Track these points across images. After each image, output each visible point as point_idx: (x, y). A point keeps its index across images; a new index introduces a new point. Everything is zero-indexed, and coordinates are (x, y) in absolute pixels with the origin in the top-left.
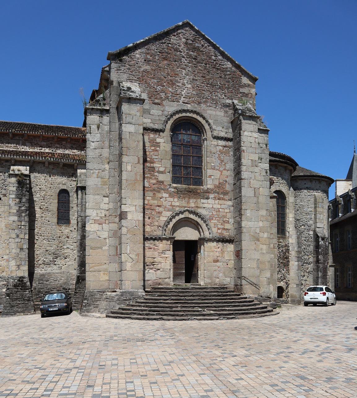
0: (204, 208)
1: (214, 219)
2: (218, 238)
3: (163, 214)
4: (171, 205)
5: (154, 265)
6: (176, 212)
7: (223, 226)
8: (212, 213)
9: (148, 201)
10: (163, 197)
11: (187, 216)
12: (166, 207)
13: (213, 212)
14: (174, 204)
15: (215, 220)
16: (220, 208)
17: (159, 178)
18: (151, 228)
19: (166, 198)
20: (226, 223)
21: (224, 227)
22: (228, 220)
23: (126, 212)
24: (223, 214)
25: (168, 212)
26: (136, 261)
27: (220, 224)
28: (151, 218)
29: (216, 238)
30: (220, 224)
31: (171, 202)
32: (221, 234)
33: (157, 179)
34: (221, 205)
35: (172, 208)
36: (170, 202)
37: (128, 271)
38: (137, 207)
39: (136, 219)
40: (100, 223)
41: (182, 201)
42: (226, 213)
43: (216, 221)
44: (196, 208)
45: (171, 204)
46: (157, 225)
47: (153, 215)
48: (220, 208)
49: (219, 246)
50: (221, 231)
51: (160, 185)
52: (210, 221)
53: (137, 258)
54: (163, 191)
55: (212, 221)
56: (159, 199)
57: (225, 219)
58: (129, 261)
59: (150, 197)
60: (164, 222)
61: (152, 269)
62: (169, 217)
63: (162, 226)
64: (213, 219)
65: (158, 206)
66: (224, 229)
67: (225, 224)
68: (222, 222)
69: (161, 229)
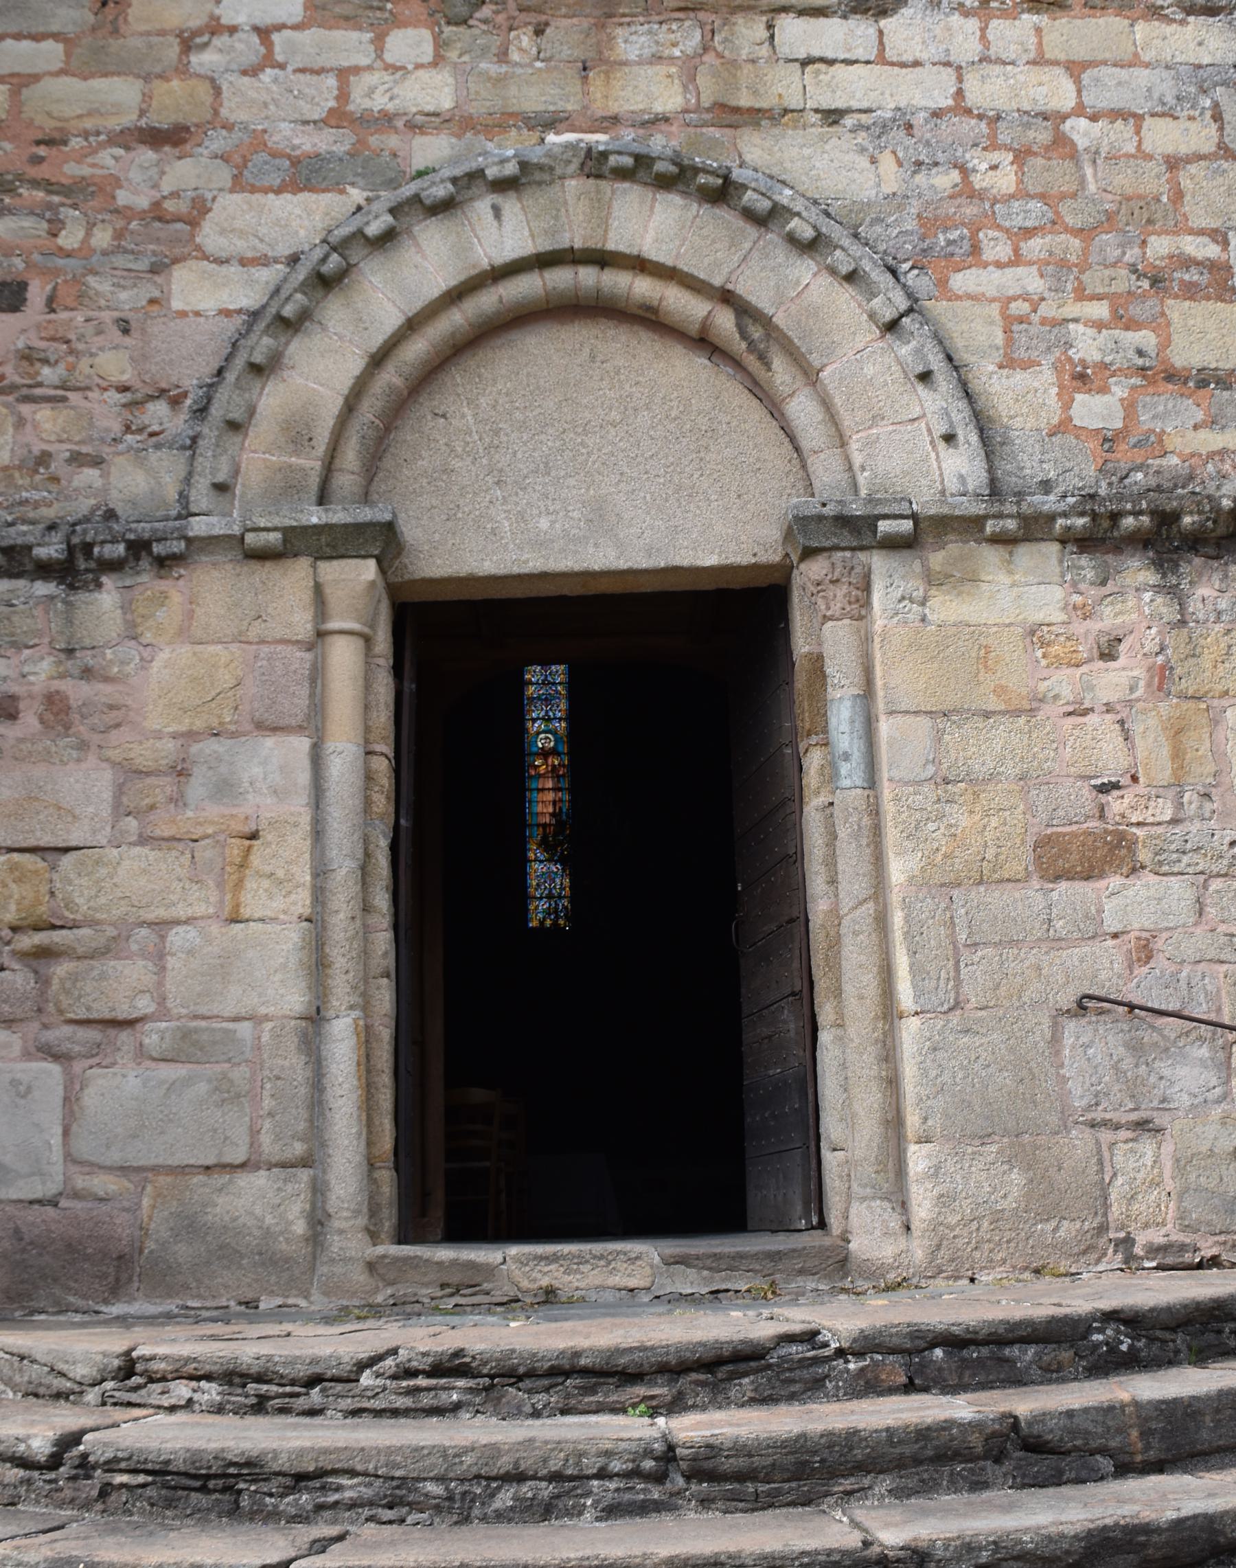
0: (833, 116)
1: (996, 247)
2: (1092, 497)
3: (210, 236)
5: (45, 953)
6: (408, 190)
7: (1146, 338)
8: (955, 176)
9: (15, 93)
10: (215, 28)
11: (576, 237)
12: (259, 141)
13: (979, 161)
14: (380, 102)
15: (1017, 260)
16: (1079, 110)
18: (20, 423)
19: (264, 33)
20: (1191, 292)
21: (1165, 343)
22: (1212, 251)
24: (1123, 180)
27: (1101, 310)
29: (1049, 503)
30: (1101, 310)
31: (344, 74)
32: (1124, 455)
34: (1075, 69)
35: (361, 142)
41: (502, 56)
42: (1173, 163)
43: (1034, 283)
44: (715, 132)
45: (343, 95)
46: (125, 378)
47: (68, 255)
48: (1079, 110)
49: (1109, 619)
50: (1130, 407)
52: (942, 283)
55: (961, 281)
56: (173, 50)
57: (1160, 247)
59: (56, 36)
62: (294, 260)
63: (190, 383)
64: (976, 249)
65: (155, 138)
66: (1171, 376)
67: (1177, 309)
68: (1124, 282)
69: (175, 423)
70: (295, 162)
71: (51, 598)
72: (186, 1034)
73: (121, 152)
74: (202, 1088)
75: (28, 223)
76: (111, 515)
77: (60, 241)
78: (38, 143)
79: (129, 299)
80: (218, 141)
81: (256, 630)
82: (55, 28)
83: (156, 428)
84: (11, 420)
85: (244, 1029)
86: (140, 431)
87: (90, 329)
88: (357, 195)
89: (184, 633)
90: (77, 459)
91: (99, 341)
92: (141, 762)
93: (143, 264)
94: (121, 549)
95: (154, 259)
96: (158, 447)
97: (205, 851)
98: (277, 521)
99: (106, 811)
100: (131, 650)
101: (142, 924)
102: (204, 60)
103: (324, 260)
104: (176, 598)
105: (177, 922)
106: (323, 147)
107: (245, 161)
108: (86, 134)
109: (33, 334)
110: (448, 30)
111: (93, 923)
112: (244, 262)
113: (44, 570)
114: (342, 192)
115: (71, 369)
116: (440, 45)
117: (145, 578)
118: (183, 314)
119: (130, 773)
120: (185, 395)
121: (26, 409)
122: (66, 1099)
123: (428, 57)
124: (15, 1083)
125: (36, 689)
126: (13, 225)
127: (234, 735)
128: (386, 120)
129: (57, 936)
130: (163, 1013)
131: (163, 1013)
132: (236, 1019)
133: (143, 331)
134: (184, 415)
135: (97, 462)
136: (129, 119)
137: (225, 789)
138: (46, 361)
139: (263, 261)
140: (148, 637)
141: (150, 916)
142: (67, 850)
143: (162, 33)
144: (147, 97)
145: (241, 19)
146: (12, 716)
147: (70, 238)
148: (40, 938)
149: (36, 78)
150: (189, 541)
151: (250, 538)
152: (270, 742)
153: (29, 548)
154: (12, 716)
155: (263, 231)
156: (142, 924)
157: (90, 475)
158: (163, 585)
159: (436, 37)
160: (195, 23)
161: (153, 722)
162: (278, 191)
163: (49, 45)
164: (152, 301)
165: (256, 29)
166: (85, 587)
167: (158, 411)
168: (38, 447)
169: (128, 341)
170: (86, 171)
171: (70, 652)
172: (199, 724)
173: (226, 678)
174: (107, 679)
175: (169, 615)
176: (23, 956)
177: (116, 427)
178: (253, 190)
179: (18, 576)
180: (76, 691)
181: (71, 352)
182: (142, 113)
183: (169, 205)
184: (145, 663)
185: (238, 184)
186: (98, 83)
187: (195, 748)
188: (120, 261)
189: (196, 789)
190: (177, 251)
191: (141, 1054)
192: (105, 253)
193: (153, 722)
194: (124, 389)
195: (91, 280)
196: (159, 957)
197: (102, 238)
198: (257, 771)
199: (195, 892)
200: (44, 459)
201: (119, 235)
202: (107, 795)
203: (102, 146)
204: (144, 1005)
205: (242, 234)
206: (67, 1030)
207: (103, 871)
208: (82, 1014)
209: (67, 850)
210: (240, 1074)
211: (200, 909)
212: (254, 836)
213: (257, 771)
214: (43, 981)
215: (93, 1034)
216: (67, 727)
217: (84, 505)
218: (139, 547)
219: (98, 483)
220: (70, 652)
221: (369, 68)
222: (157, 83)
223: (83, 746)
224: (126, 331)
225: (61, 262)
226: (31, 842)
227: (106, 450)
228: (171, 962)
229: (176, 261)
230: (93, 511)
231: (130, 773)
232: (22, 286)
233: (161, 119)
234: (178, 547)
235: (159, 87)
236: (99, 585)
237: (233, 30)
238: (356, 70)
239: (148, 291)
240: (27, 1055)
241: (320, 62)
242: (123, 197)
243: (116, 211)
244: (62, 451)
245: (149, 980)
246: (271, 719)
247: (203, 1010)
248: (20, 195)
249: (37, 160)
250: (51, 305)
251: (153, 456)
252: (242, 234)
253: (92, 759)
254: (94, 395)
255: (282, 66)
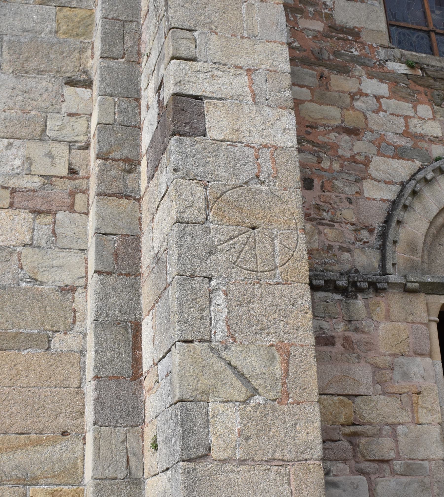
3: (372, 171)
4: (406, 133)
5: (355, 434)
10: (361, 93)
12: (382, 138)
14: (419, 130)
17: (336, 16)
18: (320, 233)
19: (378, 98)
23: (196, 97)
25: (396, 163)
26: (272, 395)
28: (317, 183)
31: (406, 118)
33: (329, 17)
36: (402, 120)
37: (224, 461)
38: (259, 79)
39: (256, 139)
40: (44, 207)
45: (407, 126)
46: (354, 220)
51: (342, 43)
53: (279, 372)
54: (359, 70)
58: (224, 393)
59: (307, 87)
60: (387, 205)
61: (345, 461)
62: (403, 185)
70: (396, 148)
71: (341, 300)
72: (408, 465)
73: (337, 135)
74: (416, 485)
75: (310, 156)
76: (357, 271)
77: (322, 165)
78: (308, 126)
79: (350, 190)
80: (368, 136)
81: (410, 318)
82: (306, 84)
83: (365, 240)
84: (316, 231)
85: (426, 463)
86: (361, 240)
87: (338, 200)
88: (418, 164)
89: (387, 318)
90: (342, 249)
91: (341, 205)
92: (381, 365)
93: (352, 178)
94: (322, 282)
95: (355, 177)
96: (369, 247)
97: (405, 398)
98: (417, 280)
99: (370, 383)
100: (369, 322)
101: (387, 424)
102: (358, 104)
103: (415, 186)
104: (383, 304)
105: (399, 424)
106: (404, 144)
107: (380, 145)
108: (324, 126)
109: (317, 199)
110: (436, 107)
111: (371, 424)
112: (386, 182)
113: (337, 289)
114: (413, 161)
115: (334, 214)
116: (434, 112)
117: (371, 296)
118: (369, 199)
119: (377, 368)
120: (374, 229)
121: (321, 228)
122: (370, 490)
123: (431, 117)
124: (352, 483)
125: (340, 334)
126: (304, 157)
127: (408, 356)
128: (421, 137)
129: (359, 428)
130: (398, 458)
131: (398, 458)
132: (423, 460)
133: (356, 203)
134: (375, 237)
135: (349, 251)
136: (338, 123)
137: (406, 375)
138: (324, 210)
139: (391, 183)
140: (375, 318)
141: (390, 422)
142: (356, 396)
143: (343, 92)
144: (342, 115)
145: (369, 92)
146: (333, 344)
147: (325, 164)
148: (352, 429)
149: (303, 102)
150: (388, 283)
151: (409, 285)
152: (419, 359)
153: (335, 281)
154: (333, 344)
155: (390, 172)
156: (387, 424)
157: (347, 255)
158: (378, 299)
159: (432, 109)
160: (354, 90)
161: (382, 350)
162: (393, 158)
163: (304, 89)
164: (357, 193)
165: (375, 96)
166: (351, 297)
167: (364, 234)
168: (327, 243)
169: (351, 206)
170: (327, 140)
171: (350, 321)
172: (397, 352)
173: (404, 335)
174: (363, 332)
175: (381, 310)
176: (345, 435)
177: (353, 239)
178: (384, 156)
179: (328, 291)
180: (355, 336)
181: (333, 208)
182: (342, 122)
183: (357, 157)
184: (377, 328)
185: (379, 154)
186: (325, 107)
187: (396, 360)
188: (345, 176)
189: (397, 375)
190: (362, 175)
191: (393, 472)
192: (338, 172)
193: (382, 350)
194: (353, 224)
195: (335, 181)
196: (395, 436)
197: (336, 166)
198: (416, 369)
199: (404, 414)
200: (330, 247)
201: (342, 166)
202: (370, 376)
203: (330, 132)
204: (392, 455)
205: (383, 172)
206: (368, 464)
207: (372, 404)
208: (373, 458)
209: (356, 396)
210: (427, 480)
211: (407, 420)
212: (419, 393)
213: (416, 369)
214: (355, 446)
215: (375, 465)
216: (353, 350)
217: (347, 267)
218: (373, 285)
219: (350, 259)
220: (350, 321)
221: (413, 117)
222: (345, 111)
223: (359, 357)
224: (351, 203)
225: (323, 173)
226: (346, 392)
227: (351, 247)
228: (400, 439)
229: (363, 179)
230: (351, 269)
231: (377, 368)
232: (312, 181)
233: (351, 125)
234: (385, 285)
235: (347, 113)
236: (357, 297)
237: (367, 95)
238: (410, 117)
239: (355, 189)
240: (352, 473)
241: (398, 112)
242: (340, 152)
243: (339, 157)
244: (336, 245)
245: (393, 445)
246: (419, 351)
247: (412, 457)
248: (304, 145)
249: (309, 133)
250: (323, 189)
251: (368, 251)
252: (383, 172)
253: (363, 363)
254: (343, 225)
255: (385, 112)
